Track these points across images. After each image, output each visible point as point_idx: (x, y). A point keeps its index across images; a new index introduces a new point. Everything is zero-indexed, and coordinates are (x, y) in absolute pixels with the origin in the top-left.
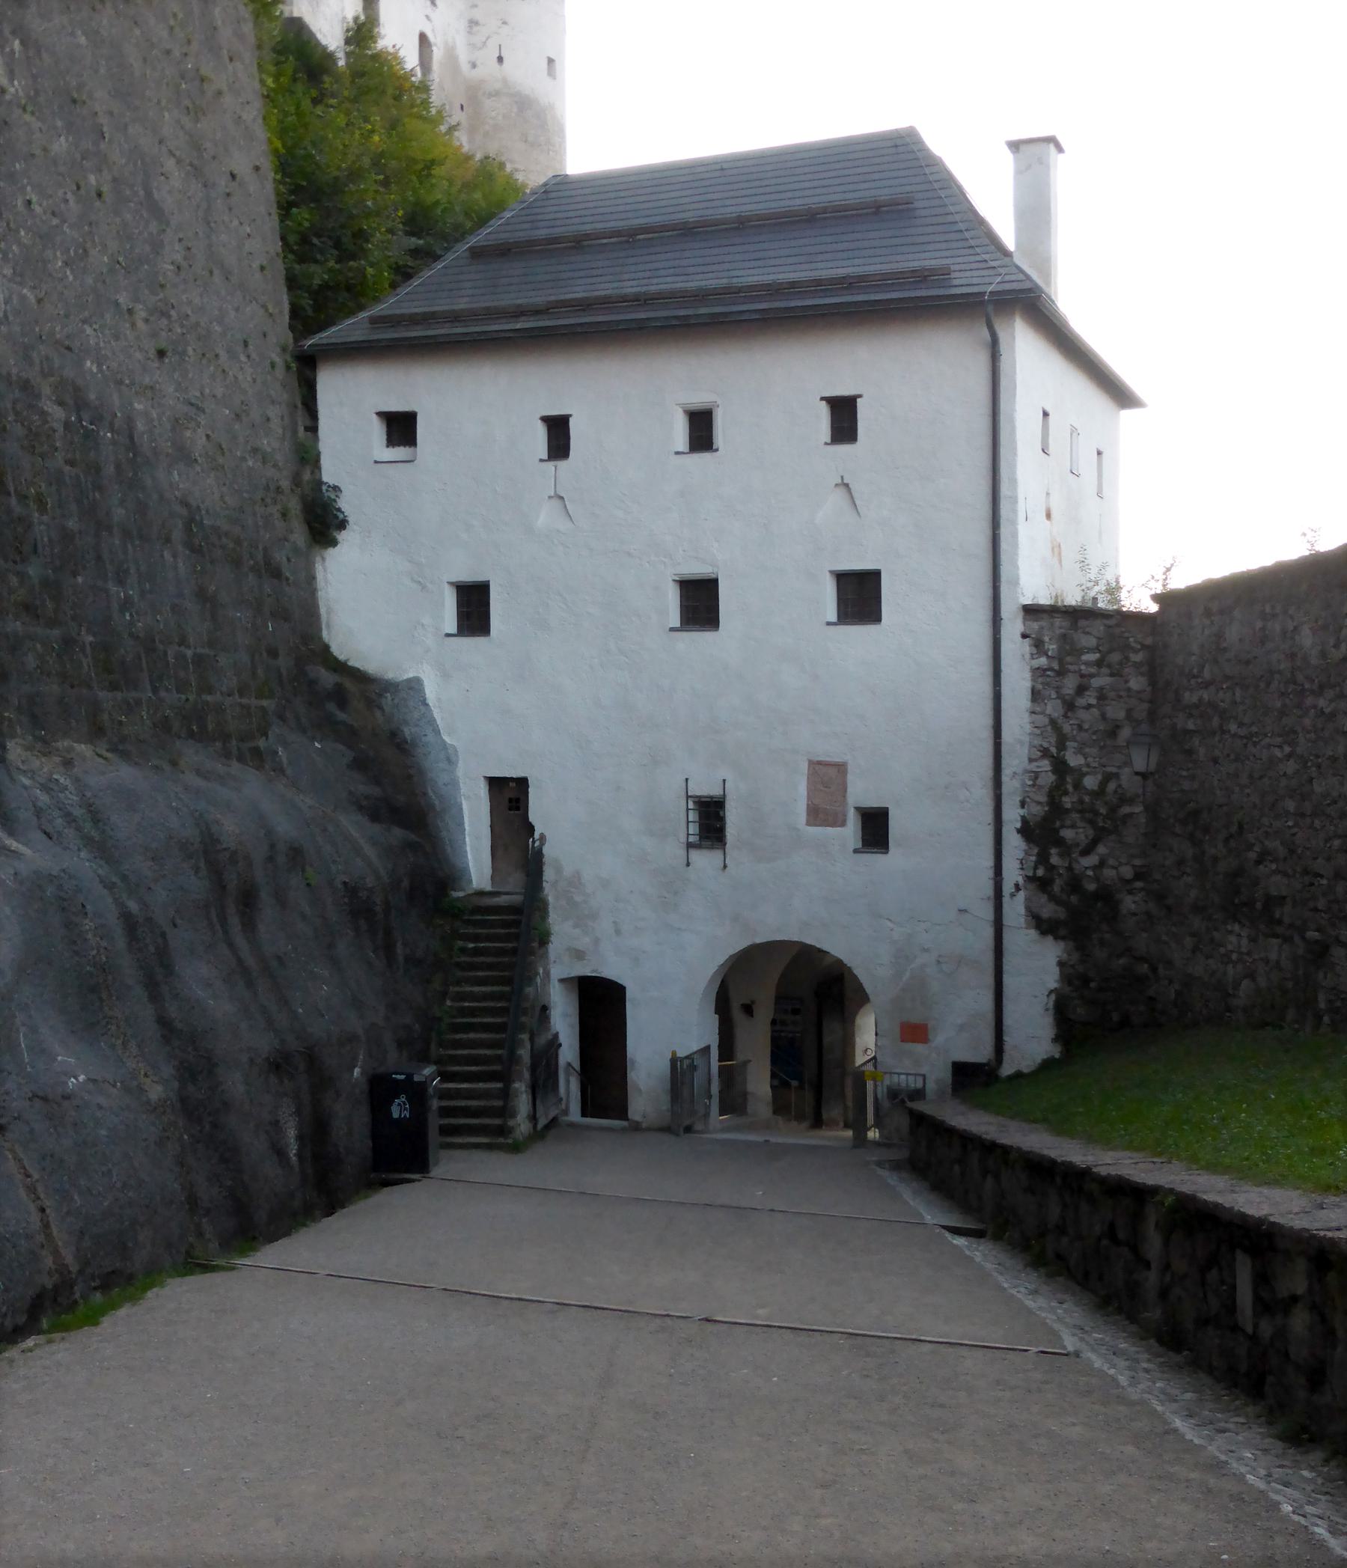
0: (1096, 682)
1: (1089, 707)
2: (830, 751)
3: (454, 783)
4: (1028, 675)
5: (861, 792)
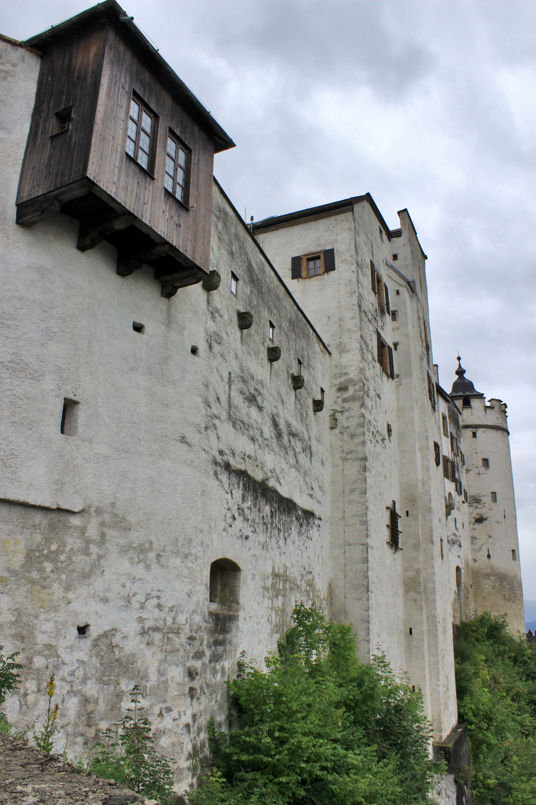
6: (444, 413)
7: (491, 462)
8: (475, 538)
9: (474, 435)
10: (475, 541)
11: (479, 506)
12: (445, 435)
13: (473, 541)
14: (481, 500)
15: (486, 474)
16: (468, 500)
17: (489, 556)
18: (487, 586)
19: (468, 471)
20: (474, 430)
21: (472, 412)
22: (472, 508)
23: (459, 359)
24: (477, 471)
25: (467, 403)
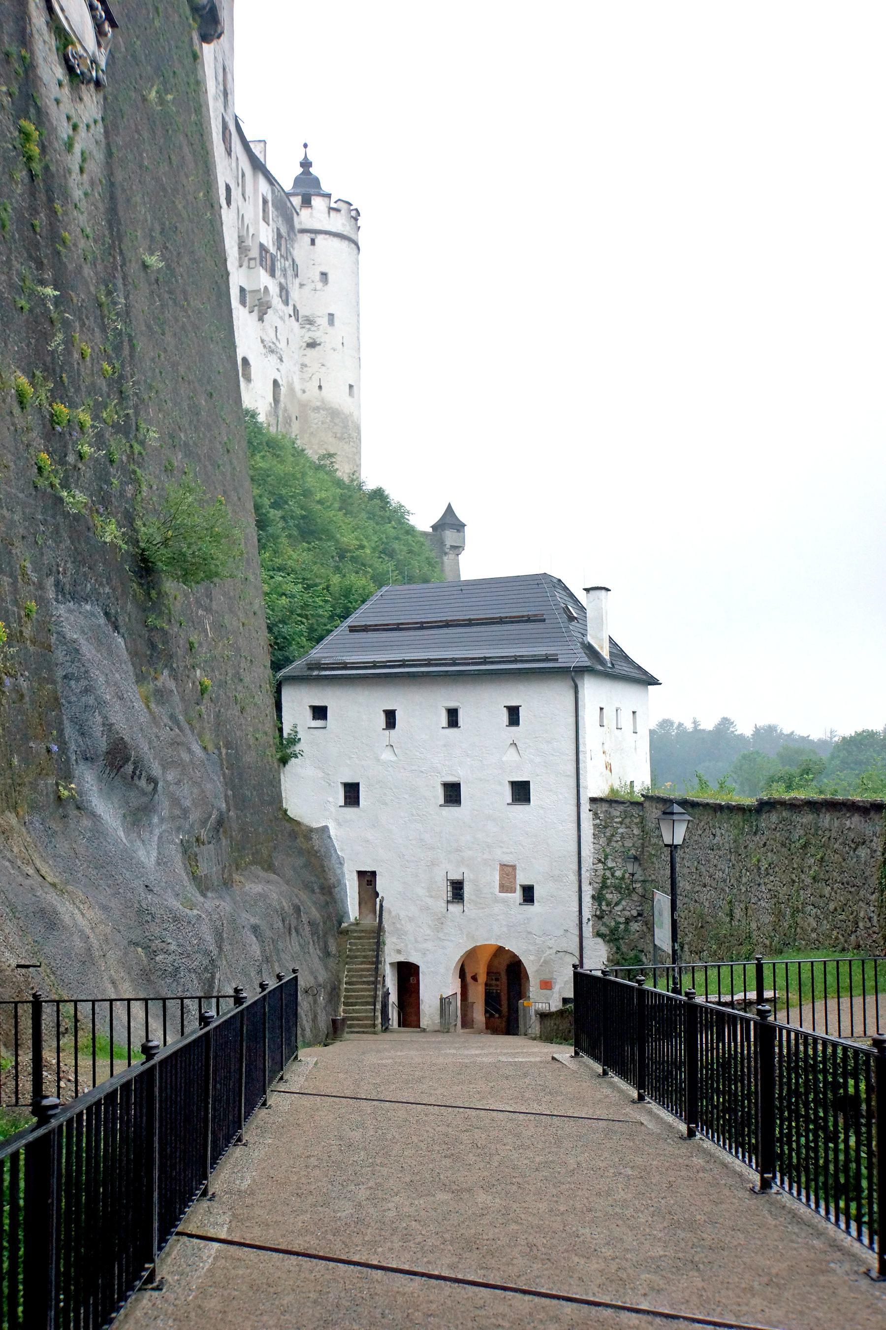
0: (620, 831)
1: (617, 841)
2: (508, 859)
3: (343, 874)
4: (592, 827)
5: (522, 879)
8: (306, 366)
9: (313, 242)
10: (305, 369)
11: (313, 328)
12: (264, 220)
16: (300, 320)
17: (320, 387)
18: (316, 421)
19: (301, 285)
20: (313, 236)
21: (311, 213)
22: (304, 330)
23: (305, 146)
24: (312, 286)
25: (307, 202)
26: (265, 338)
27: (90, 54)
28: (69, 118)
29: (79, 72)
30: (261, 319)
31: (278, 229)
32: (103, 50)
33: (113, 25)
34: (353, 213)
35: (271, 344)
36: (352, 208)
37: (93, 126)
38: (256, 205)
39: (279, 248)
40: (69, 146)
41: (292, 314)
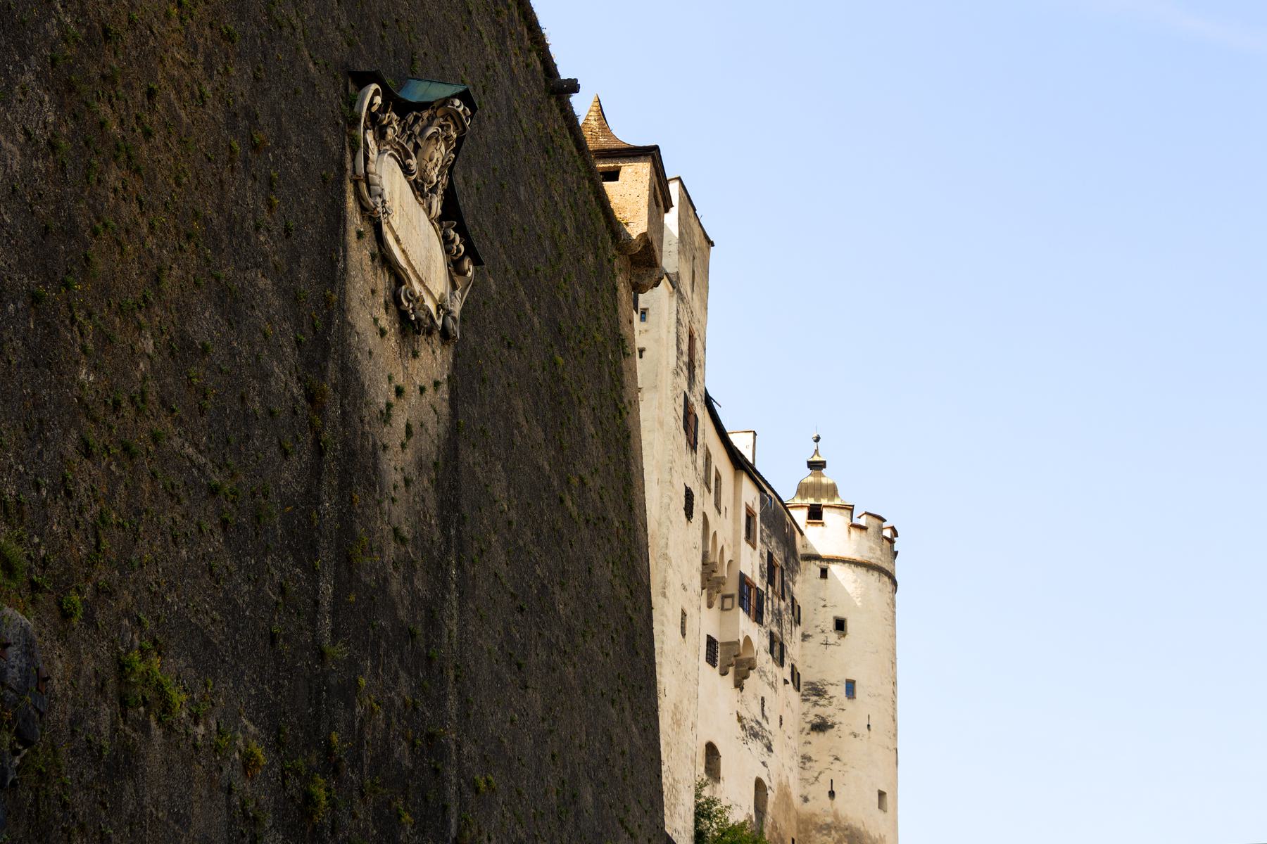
6: (751, 505)
7: (850, 626)
8: (810, 759)
9: (824, 573)
10: (808, 765)
11: (821, 702)
13: (804, 763)
14: (825, 692)
15: (840, 645)
16: (802, 690)
17: (832, 794)
19: (805, 637)
20: (824, 564)
22: (808, 704)
23: (817, 439)
24: (821, 638)
26: (744, 713)
27: (437, 297)
28: (390, 378)
29: (413, 318)
30: (739, 685)
31: (770, 555)
32: (458, 293)
33: (477, 262)
34: (887, 533)
35: (753, 724)
36: (885, 525)
37: (430, 390)
38: (736, 519)
39: (771, 581)
40: (386, 416)
41: (789, 679)
